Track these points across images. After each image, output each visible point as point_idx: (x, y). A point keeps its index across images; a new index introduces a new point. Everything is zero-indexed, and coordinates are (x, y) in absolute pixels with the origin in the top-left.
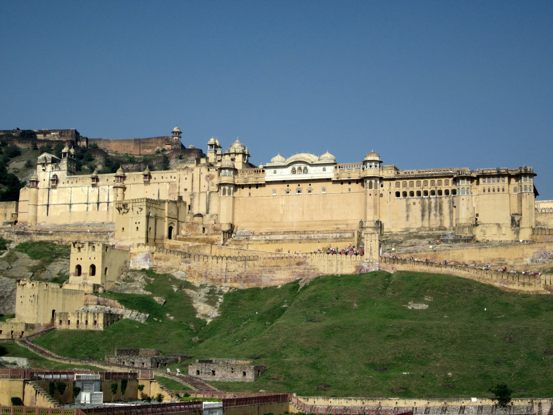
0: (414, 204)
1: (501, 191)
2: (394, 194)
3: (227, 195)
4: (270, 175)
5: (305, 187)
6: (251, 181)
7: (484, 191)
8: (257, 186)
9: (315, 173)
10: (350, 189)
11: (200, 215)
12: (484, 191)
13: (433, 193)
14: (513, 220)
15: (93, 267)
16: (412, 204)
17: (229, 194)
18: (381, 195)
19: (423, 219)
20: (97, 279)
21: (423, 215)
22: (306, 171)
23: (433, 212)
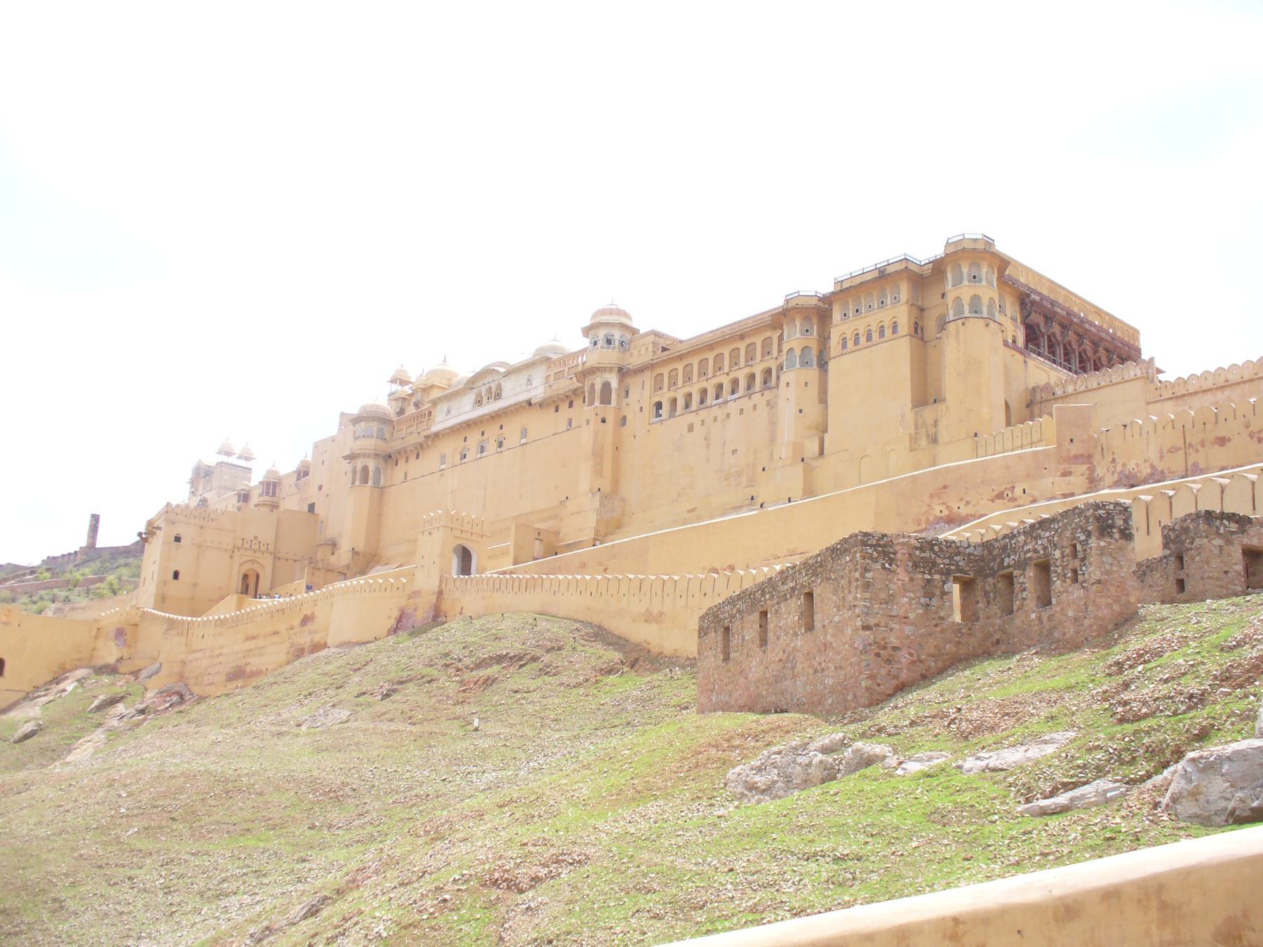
0: (691, 428)
1: (888, 332)
2: (649, 409)
3: (357, 483)
4: (441, 421)
5: (492, 433)
6: (414, 439)
7: (844, 346)
8: (419, 450)
9: (514, 393)
10: (570, 422)
12: (844, 346)
16: (686, 430)
17: (365, 480)
18: (624, 420)
22: (498, 396)
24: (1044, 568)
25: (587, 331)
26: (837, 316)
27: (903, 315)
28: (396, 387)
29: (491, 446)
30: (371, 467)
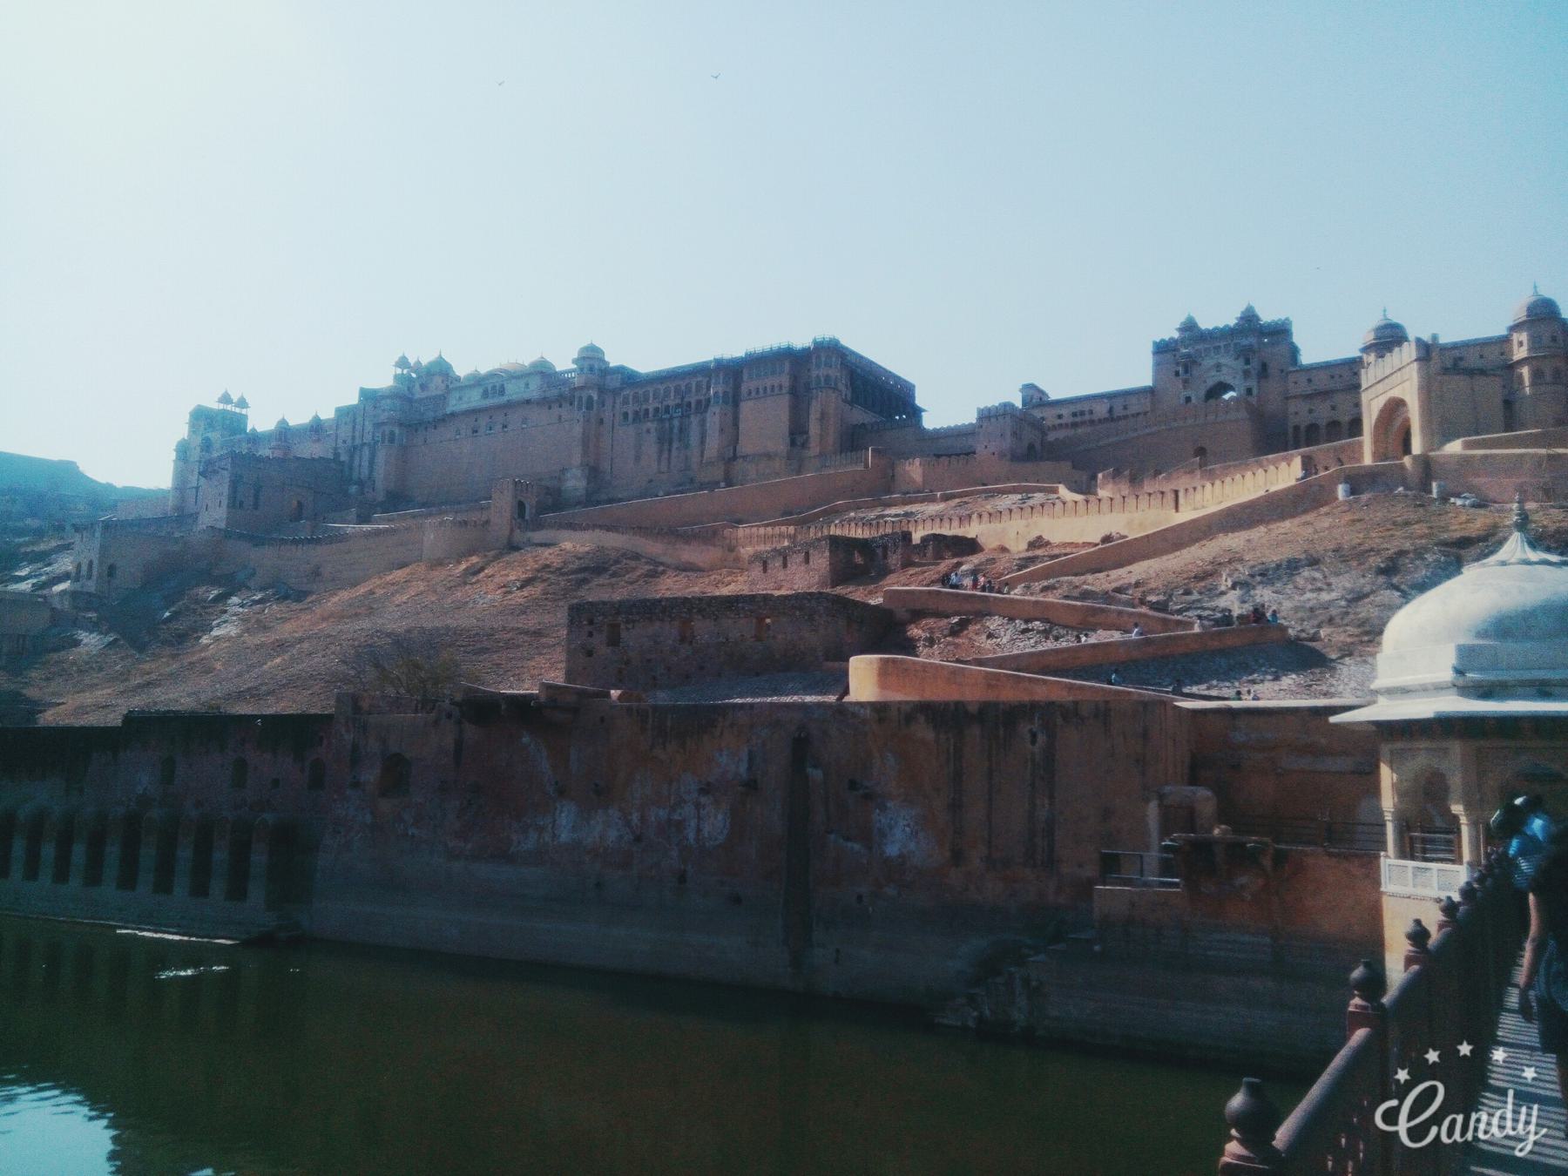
0: (648, 431)
2: (619, 418)
4: (454, 405)
6: (430, 415)
9: (514, 391)
11: (361, 483)
13: (678, 406)
14: (793, 443)
15: (91, 563)
17: (392, 440)
18: (601, 421)
19: (659, 461)
20: (91, 586)
21: (661, 452)
22: (502, 391)
23: (675, 445)
24: (885, 548)
25: (575, 361)
26: (745, 377)
27: (785, 380)
28: (399, 371)
29: (498, 427)
30: (397, 431)
